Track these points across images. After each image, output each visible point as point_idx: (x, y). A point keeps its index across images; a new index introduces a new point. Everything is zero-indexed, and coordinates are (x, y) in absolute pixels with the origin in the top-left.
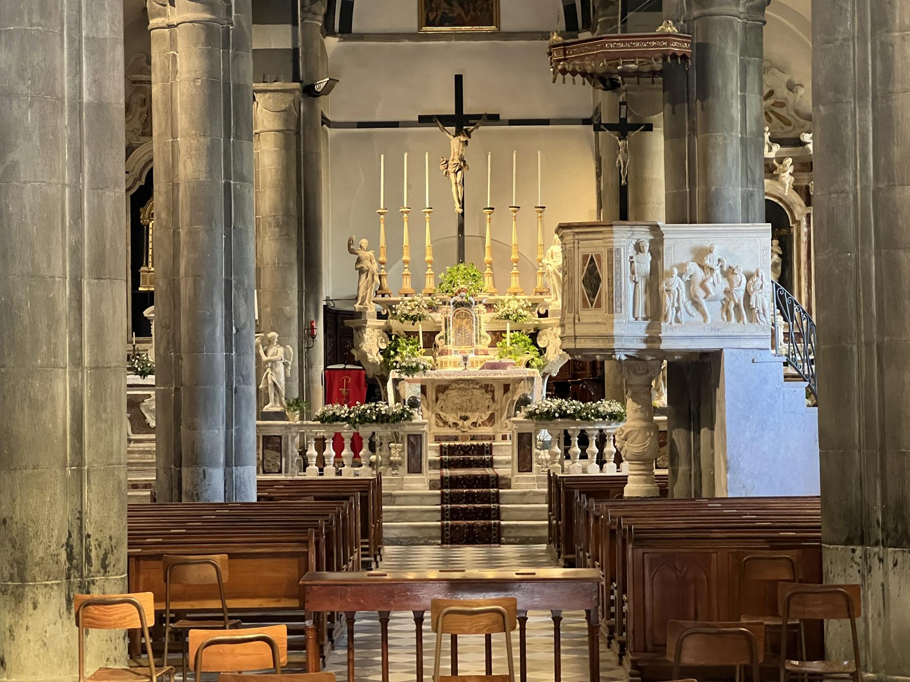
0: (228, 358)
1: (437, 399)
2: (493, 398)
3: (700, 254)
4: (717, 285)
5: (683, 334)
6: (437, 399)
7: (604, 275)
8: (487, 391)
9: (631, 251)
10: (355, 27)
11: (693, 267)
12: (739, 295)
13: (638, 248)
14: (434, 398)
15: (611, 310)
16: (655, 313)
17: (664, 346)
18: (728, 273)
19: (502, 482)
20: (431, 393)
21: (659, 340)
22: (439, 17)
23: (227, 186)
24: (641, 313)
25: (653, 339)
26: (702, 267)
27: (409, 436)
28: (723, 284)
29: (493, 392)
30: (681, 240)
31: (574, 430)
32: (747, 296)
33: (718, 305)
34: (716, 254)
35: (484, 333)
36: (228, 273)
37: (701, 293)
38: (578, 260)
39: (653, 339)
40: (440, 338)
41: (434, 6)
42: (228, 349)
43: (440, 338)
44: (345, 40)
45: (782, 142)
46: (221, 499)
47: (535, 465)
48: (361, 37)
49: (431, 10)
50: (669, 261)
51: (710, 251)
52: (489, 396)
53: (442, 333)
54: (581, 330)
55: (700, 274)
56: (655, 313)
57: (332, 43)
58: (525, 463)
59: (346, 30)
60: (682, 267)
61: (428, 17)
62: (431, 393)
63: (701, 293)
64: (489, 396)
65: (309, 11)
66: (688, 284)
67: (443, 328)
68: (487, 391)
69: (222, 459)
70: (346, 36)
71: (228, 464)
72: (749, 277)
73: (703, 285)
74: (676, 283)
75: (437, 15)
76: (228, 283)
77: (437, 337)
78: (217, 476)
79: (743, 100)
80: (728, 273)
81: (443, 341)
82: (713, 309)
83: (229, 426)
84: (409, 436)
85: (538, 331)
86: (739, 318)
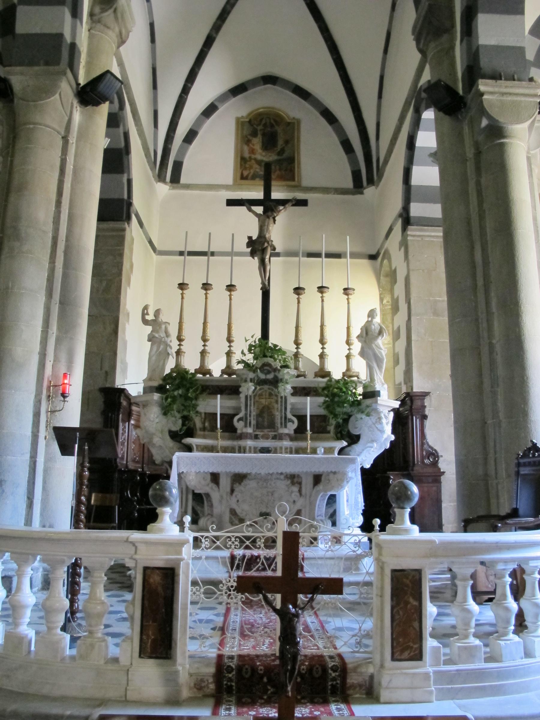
1: (232, 491)
2: (300, 491)
6: (232, 491)
8: (293, 483)
14: (229, 489)
19: (352, 679)
20: (225, 482)
22: (251, 174)
27: (146, 569)
29: (300, 483)
31: (506, 561)
35: (289, 416)
40: (239, 420)
41: (247, 166)
43: (239, 420)
44: (174, 188)
47: (430, 643)
48: (187, 187)
49: (245, 169)
52: (295, 489)
53: (241, 415)
57: (163, 189)
58: (407, 641)
61: (242, 175)
62: (225, 482)
64: (295, 489)
65: (99, 21)
67: (243, 409)
68: (293, 483)
70: (175, 185)
75: (250, 173)
77: (236, 419)
81: (242, 423)
84: (146, 569)
85: (350, 416)
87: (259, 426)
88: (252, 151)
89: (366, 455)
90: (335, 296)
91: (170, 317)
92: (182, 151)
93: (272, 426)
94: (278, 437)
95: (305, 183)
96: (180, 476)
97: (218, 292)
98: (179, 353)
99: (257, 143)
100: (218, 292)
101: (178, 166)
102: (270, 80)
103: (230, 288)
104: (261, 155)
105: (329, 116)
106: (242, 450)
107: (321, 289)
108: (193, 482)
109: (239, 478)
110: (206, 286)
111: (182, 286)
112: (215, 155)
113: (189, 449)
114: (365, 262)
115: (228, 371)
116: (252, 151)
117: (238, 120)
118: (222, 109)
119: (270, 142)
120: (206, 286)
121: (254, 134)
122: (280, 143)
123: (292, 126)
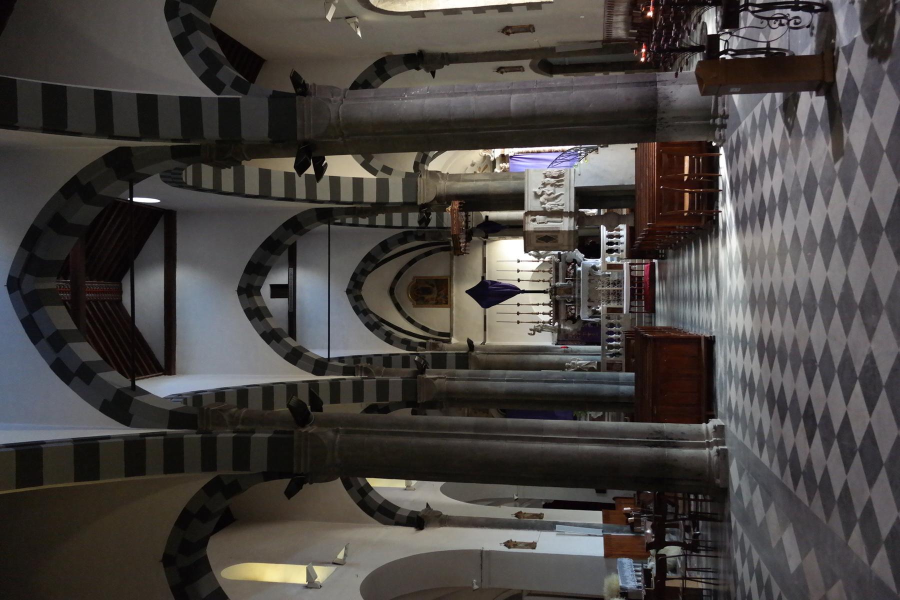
0: (575, 382)
3: (537, 196)
4: (549, 189)
5: (567, 202)
7: (545, 234)
9: (535, 223)
10: (448, 331)
11: (542, 199)
12: (553, 181)
13: (534, 220)
15: (559, 231)
16: (560, 214)
17: (573, 210)
18: (545, 185)
21: (571, 212)
23: (507, 381)
24: (560, 219)
25: (570, 214)
26: (541, 195)
28: (549, 187)
30: (531, 204)
32: (553, 177)
33: (557, 189)
34: (537, 190)
36: (542, 381)
37: (552, 196)
38: (538, 245)
39: (570, 214)
42: (572, 382)
45: (494, 167)
46: (633, 387)
48: (451, 329)
50: (539, 208)
51: (535, 193)
54: (566, 243)
55: (545, 196)
56: (560, 214)
57: (454, 340)
59: (449, 335)
60: (542, 203)
62: (591, 304)
63: (552, 196)
66: (548, 200)
69: (616, 386)
71: (618, 384)
72: (546, 177)
73: (549, 195)
74: (548, 205)
76: (546, 381)
78: (624, 388)
79: (477, 181)
80: (545, 185)
82: (558, 191)
83: (603, 383)
86: (562, 181)
87: (571, 293)
88: (432, 299)
89: (580, 255)
90: (520, 266)
91: (532, 326)
92: (433, 332)
93: (571, 289)
94: (574, 287)
95: (448, 274)
96: (590, 317)
97: (520, 309)
98: (544, 322)
99: (427, 297)
100: (520, 309)
101: (441, 334)
102: (392, 292)
103: (518, 305)
104: (434, 296)
105: (411, 263)
106: (579, 299)
107: (518, 271)
108: (590, 313)
109: (589, 300)
110: (518, 313)
111: (518, 322)
112: (435, 318)
113: (579, 317)
114: (487, 246)
115: (549, 305)
116: (432, 299)
117: (415, 307)
118: (409, 315)
119: (428, 291)
120: (518, 313)
121: (423, 299)
122: (427, 286)
123: (418, 281)
